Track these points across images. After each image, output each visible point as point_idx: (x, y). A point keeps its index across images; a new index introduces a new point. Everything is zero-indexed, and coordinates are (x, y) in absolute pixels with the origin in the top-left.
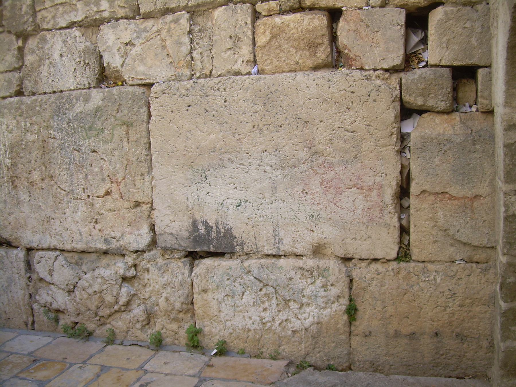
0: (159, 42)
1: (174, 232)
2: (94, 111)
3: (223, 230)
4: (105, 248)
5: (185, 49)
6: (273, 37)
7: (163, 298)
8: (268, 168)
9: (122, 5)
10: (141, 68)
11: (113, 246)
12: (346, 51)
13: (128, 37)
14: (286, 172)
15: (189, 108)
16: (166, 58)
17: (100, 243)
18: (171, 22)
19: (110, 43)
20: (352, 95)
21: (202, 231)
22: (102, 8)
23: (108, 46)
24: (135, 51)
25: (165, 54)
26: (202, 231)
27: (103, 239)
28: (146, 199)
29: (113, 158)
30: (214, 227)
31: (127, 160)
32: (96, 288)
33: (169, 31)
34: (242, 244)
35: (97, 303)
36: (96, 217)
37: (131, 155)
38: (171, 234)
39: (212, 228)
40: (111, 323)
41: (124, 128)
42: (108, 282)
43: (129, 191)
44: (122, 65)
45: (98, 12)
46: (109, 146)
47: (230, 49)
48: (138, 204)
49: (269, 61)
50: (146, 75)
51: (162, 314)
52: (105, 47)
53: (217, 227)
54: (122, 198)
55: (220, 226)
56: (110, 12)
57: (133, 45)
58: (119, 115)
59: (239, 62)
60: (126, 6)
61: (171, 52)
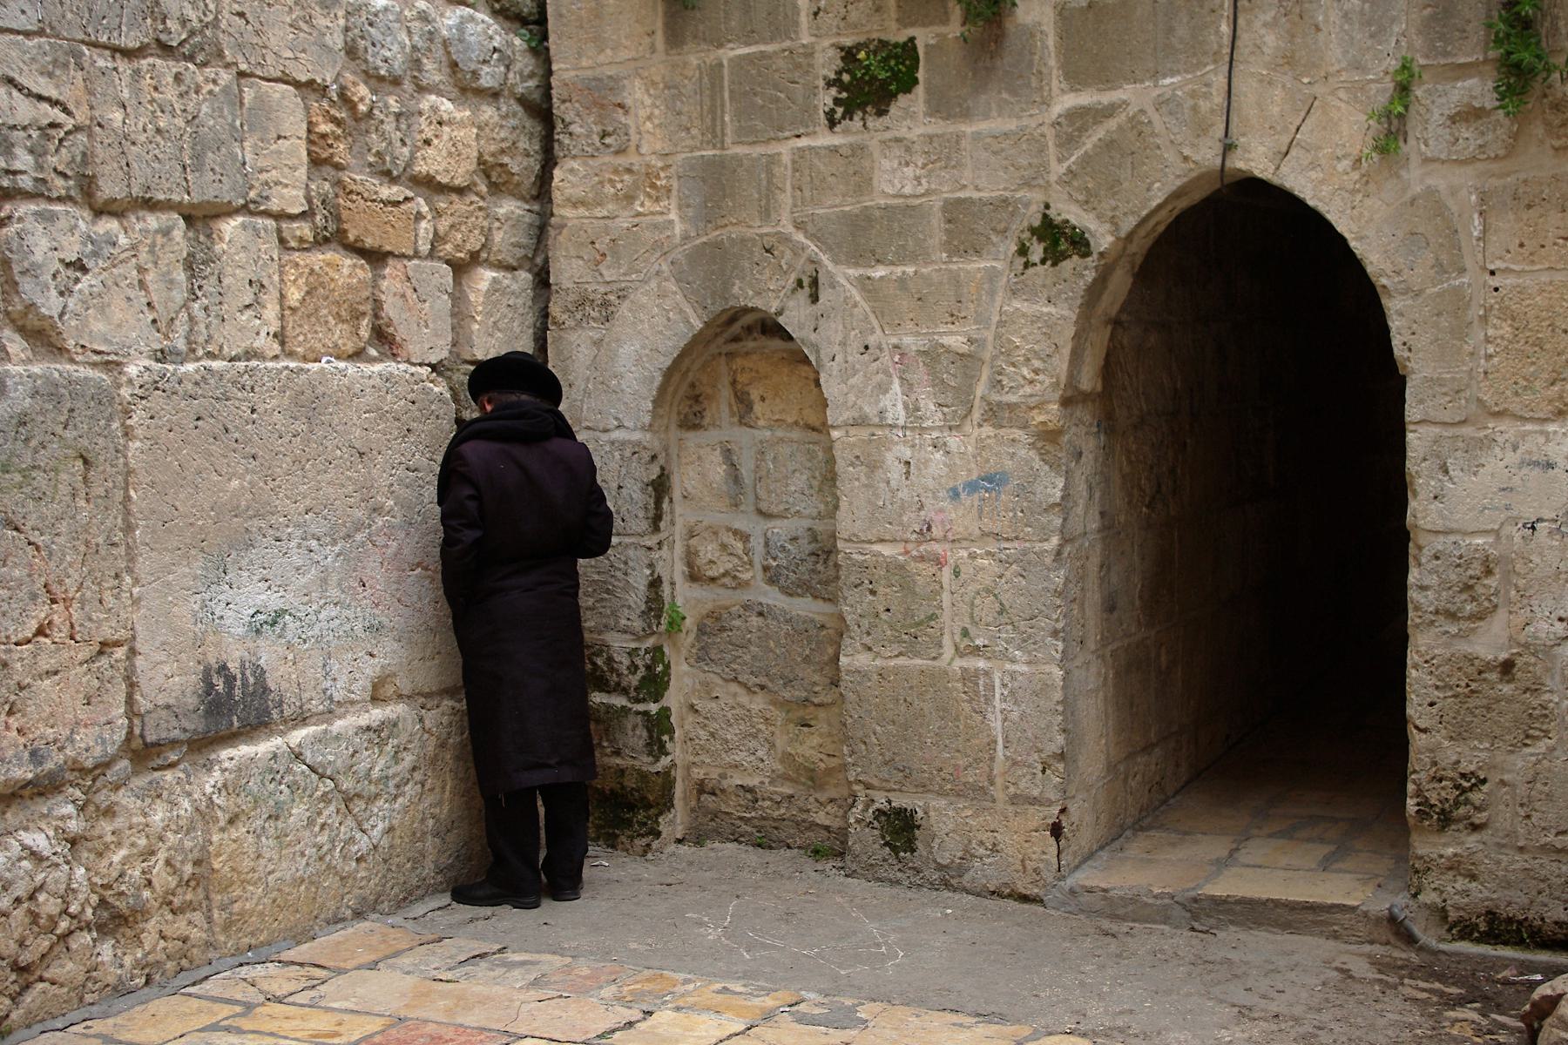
0: (135, 272)
1: (172, 701)
2: (14, 421)
3: (252, 680)
4: (30, 776)
5: (179, 296)
6: (308, 293)
7: (161, 863)
8: (314, 543)
9: (60, 168)
10: (98, 326)
11: (49, 766)
12: (391, 330)
13: (77, 247)
14: (337, 549)
15: (200, 423)
16: (145, 309)
17: (20, 766)
18: (157, 232)
19: (38, 257)
20: (413, 408)
21: (220, 687)
22: (17, 165)
23: (33, 264)
24: (86, 281)
25: (144, 301)
26: (220, 687)
27: (26, 754)
28: (122, 634)
29: (56, 539)
30: (239, 676)
31: (87, 544)
32: (21, 890)
33: (152, 252)
34: (281, 703)
35: (20, 930)
36: (13, 698)
37: (94, 530)
38: (168, 707)
39: (235, 679)
40: (46, 975)
41: (80, 463)
42: (46, 864)
43: (90, 619)
44: (61, 315)
45: (8, 172)
46: (50, 510)
47: (247, 307)
48: (105, 647)
49: (301, 338)
50: (110, 343)
51: (157, 905)
52: (26, 264)
53: (243, 674)
54: (72, 638)
55: (248, 673)
56: (36, 180)
57: (84, 270)
58: (69, 434)
59: (263, 334)
60: (69, 173)
61: (155, 298)
